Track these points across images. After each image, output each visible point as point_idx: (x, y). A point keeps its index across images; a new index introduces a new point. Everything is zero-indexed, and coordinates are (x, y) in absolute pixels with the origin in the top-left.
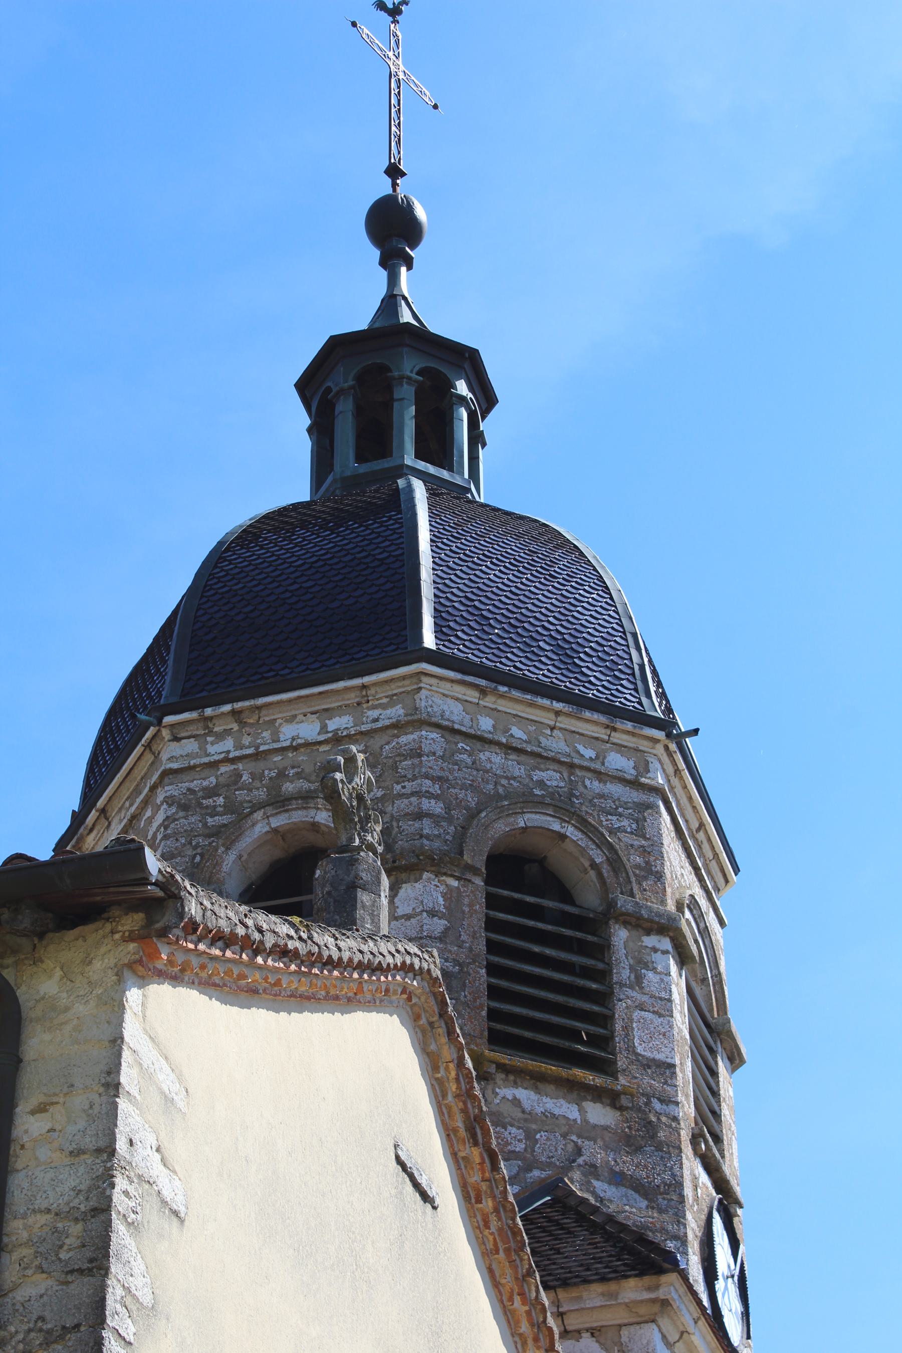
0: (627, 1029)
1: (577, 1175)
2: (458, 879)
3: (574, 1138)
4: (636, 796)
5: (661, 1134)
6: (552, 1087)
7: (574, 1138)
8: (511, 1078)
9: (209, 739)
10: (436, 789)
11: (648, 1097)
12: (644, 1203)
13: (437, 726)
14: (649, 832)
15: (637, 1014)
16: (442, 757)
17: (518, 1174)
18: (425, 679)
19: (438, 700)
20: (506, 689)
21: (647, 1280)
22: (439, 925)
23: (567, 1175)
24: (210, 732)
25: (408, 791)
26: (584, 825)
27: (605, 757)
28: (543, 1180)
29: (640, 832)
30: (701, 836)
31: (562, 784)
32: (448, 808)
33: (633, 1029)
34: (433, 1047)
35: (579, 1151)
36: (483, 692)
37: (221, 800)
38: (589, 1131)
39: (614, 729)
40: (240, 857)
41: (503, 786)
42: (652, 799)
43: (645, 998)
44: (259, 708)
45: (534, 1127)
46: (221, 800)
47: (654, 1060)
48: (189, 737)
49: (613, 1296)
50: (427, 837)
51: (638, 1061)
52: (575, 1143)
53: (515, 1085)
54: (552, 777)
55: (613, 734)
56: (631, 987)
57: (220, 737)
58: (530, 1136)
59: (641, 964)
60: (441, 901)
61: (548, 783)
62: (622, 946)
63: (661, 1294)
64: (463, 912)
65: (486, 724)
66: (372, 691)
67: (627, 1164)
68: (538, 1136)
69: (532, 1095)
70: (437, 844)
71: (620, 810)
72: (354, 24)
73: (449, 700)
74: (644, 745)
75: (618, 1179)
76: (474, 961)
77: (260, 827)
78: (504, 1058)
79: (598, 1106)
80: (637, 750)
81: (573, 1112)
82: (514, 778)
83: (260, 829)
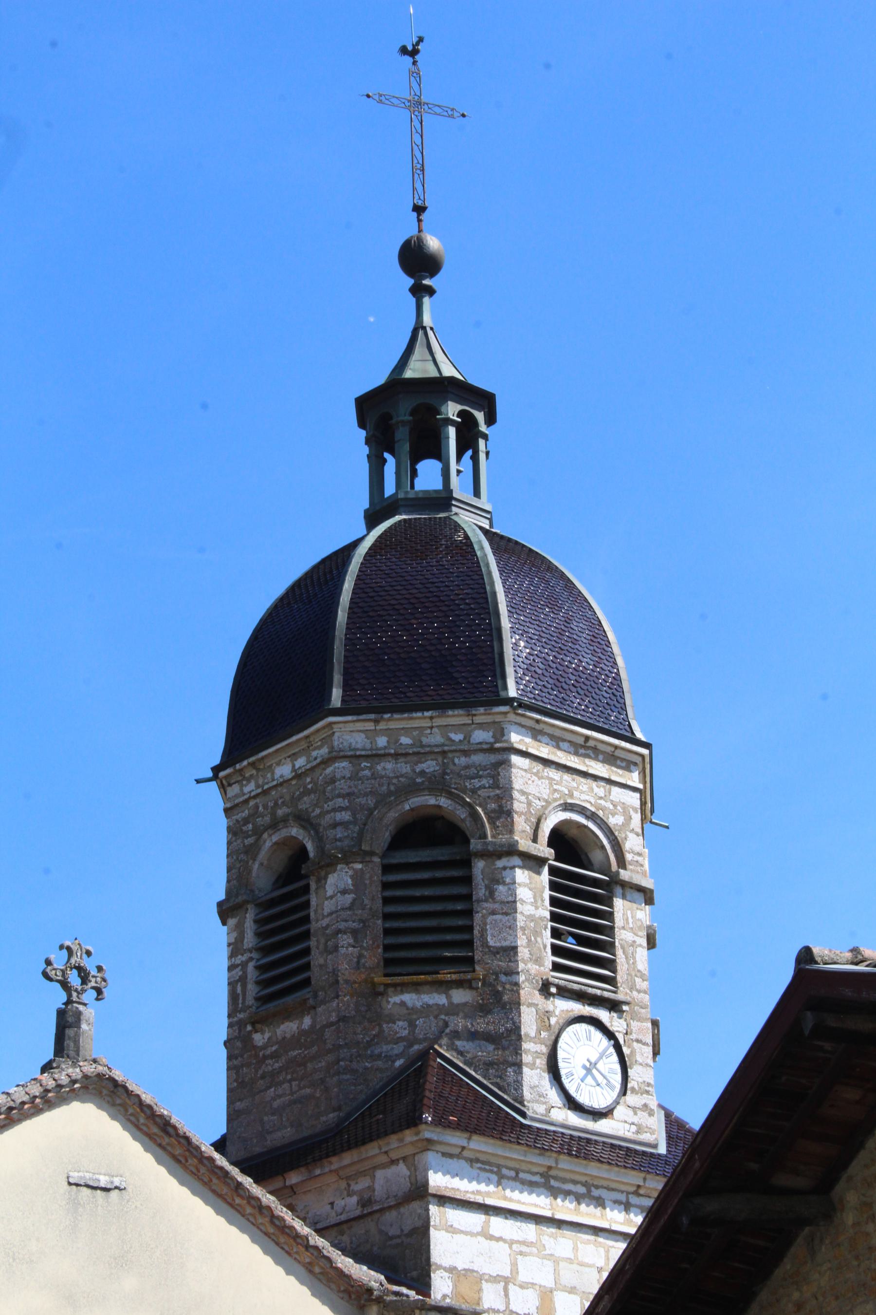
0: (483, 931)
1: (444, 1041)
2: (361, 862)
3: (443, 1017)
4: (493, 758)
5: (506, 998)
6: (428, 987)
7: (443, 1017)
8: (399, 989)
9: (244, 782)
10: (346, 803)
11: (497, 974)
12: (491, 1047)
13: (345, 757)
14: (502, 781)
15: (490, 919)
16: (350, 778)
17: (404, 1051)
18: (335, 726)
19: (347, 737)
20: (389, 715)
21: (413, 1130)
22: (349, 898)
23: (436, 1043)
24: (244, 778)
25: (329, 808)
26: (450, 795)
27: (470, 736)
28: (419, 1050)
29: (496, 785)
30: (591, 743)
31: (437, 768)
32: (354, 815)
33: (486, 930)
34: (118, 1101)
35: (446, 1024)
36: (377, 722)
37: (250, 826)
38: (453, 1010)
39: (475, 715)
40: (261, 864)
41: (394, 784)
42: (505, 757)
43: (497, 906)
44: (263, 758)
45: (414, 1017)
46: (250, 826)
47: (502, 947)
48: (235, 783)
49: (401, 1140)
50: (340, 840)
51: (490, 951)
52: (444, 1020)
53: (402, 992)
54: (430, 766)
55: (474, 718)
56: (486, 901)
57: (249, 780)
58: (412, 1025)
59: (495, 880)
60: (350, 881)
61: (427, 771)
62: (480, 874)
63: (421, 1136)
64: (366, 884)
65: (382, 741)
66: (311, 739)
67: (481, 1025)
68: (417, 1022)
69: (414, 996)
70: (346, 842)
71: (481, 773)
72: (368, 96)
73: (354, 734)
74: (498, 718)
75: (473, 1036)
76: (373, 916)
77: (269, 840)
78: (388, 980)
79: (461, 991)
80: (494, 722)
81: (440, 999)
82: (402, 776)
83: (268, 844)
